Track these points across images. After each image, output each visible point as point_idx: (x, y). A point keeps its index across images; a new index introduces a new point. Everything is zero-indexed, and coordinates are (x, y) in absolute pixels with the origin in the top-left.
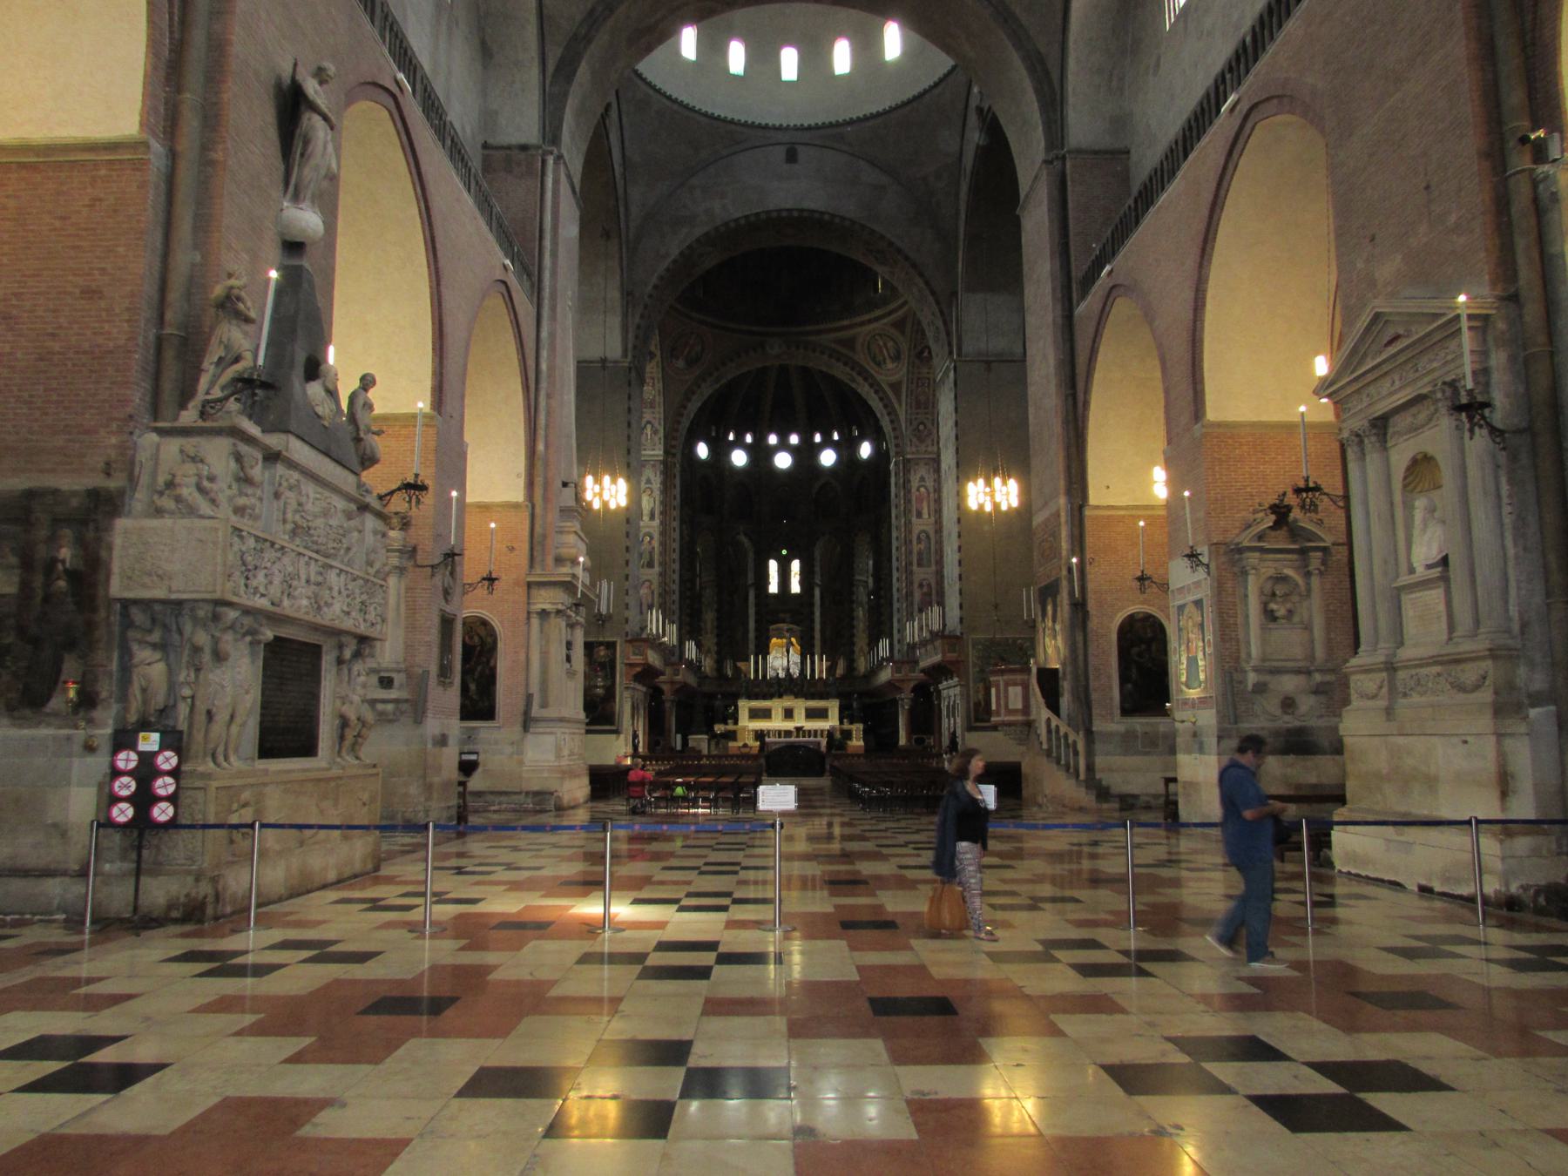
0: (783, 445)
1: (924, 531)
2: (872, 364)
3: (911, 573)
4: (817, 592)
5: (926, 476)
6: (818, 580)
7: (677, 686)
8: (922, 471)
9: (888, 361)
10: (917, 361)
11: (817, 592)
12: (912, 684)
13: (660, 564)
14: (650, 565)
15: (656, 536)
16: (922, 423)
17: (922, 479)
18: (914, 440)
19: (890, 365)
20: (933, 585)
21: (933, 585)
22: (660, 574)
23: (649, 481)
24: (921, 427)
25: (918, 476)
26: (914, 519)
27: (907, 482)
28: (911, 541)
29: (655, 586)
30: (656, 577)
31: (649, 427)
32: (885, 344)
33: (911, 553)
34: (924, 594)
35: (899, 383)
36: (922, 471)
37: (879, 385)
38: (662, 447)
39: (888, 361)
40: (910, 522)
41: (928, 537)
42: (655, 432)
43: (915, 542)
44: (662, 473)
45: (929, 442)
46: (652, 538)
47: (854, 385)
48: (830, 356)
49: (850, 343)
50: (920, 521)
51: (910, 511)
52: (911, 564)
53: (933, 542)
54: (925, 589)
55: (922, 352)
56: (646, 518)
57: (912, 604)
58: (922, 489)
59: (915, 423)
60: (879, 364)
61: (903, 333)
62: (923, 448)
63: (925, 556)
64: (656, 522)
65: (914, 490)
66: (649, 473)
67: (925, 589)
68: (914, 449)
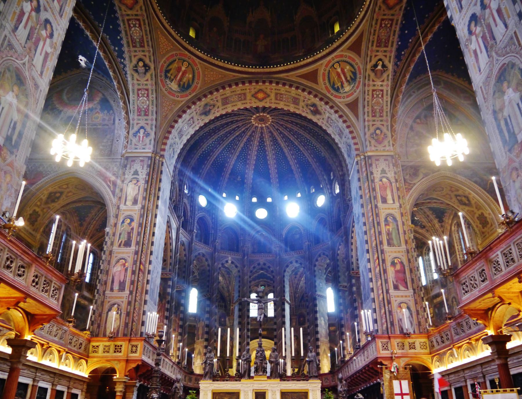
0: (262, 203)
1: (388, 215)
2: (332, 91)
3: (382, 252)
4: (287, 307)
5: (387, 169)
6: (287, 298)
7: (134, 365)
8: (382, 165)
9: (346, 84)
10: (372, 75)
11: (287, 307)
13: (138, 243)
14: (127, 244)
15: (136, 218)
16: (378, 128)
17: (383, 171)
18: (373, 142)
19: (347, 88)
20: (406, 263)
21: (406, 263)
22: (136, 253)
23: (136, 173)
24: (378, 132)
25: (380, 169)
26: (380, 204)
27: (369, 177)
28: (379, 224)
29: (129, 264)
30: (131, 255)
31: (142, 131)
32: (343, 70)
33: (380, 233)
34: (397, 272)
35: (356, 101)
36: (382, 165)
37: (338, 106)
38: (152, 146)
39: (346, 84)
40: (376, 206)
41: (395, 219)
42: (147, 135)
43: (383, 224)
44: (150, 166)
45: (386, 143)
46: (132, 220)
47: (315, 119)
48: (297, 88)
49: (313, 76)
50: (385, 206)
51: (375, 198)
52: (381, 243)
53: (400, 224)
55: (376, 66)
56: (129, 203)
57: (386, 281)
58: (384, 180)
59: (372, 129)
60: (337, 90)
61: (359, 53)
62: (380, 147)
63: (394, 236)
64: (139, 206)
65: (377, 180)
66: (137, 166)
67: (398, 267)
68: (373, 148)
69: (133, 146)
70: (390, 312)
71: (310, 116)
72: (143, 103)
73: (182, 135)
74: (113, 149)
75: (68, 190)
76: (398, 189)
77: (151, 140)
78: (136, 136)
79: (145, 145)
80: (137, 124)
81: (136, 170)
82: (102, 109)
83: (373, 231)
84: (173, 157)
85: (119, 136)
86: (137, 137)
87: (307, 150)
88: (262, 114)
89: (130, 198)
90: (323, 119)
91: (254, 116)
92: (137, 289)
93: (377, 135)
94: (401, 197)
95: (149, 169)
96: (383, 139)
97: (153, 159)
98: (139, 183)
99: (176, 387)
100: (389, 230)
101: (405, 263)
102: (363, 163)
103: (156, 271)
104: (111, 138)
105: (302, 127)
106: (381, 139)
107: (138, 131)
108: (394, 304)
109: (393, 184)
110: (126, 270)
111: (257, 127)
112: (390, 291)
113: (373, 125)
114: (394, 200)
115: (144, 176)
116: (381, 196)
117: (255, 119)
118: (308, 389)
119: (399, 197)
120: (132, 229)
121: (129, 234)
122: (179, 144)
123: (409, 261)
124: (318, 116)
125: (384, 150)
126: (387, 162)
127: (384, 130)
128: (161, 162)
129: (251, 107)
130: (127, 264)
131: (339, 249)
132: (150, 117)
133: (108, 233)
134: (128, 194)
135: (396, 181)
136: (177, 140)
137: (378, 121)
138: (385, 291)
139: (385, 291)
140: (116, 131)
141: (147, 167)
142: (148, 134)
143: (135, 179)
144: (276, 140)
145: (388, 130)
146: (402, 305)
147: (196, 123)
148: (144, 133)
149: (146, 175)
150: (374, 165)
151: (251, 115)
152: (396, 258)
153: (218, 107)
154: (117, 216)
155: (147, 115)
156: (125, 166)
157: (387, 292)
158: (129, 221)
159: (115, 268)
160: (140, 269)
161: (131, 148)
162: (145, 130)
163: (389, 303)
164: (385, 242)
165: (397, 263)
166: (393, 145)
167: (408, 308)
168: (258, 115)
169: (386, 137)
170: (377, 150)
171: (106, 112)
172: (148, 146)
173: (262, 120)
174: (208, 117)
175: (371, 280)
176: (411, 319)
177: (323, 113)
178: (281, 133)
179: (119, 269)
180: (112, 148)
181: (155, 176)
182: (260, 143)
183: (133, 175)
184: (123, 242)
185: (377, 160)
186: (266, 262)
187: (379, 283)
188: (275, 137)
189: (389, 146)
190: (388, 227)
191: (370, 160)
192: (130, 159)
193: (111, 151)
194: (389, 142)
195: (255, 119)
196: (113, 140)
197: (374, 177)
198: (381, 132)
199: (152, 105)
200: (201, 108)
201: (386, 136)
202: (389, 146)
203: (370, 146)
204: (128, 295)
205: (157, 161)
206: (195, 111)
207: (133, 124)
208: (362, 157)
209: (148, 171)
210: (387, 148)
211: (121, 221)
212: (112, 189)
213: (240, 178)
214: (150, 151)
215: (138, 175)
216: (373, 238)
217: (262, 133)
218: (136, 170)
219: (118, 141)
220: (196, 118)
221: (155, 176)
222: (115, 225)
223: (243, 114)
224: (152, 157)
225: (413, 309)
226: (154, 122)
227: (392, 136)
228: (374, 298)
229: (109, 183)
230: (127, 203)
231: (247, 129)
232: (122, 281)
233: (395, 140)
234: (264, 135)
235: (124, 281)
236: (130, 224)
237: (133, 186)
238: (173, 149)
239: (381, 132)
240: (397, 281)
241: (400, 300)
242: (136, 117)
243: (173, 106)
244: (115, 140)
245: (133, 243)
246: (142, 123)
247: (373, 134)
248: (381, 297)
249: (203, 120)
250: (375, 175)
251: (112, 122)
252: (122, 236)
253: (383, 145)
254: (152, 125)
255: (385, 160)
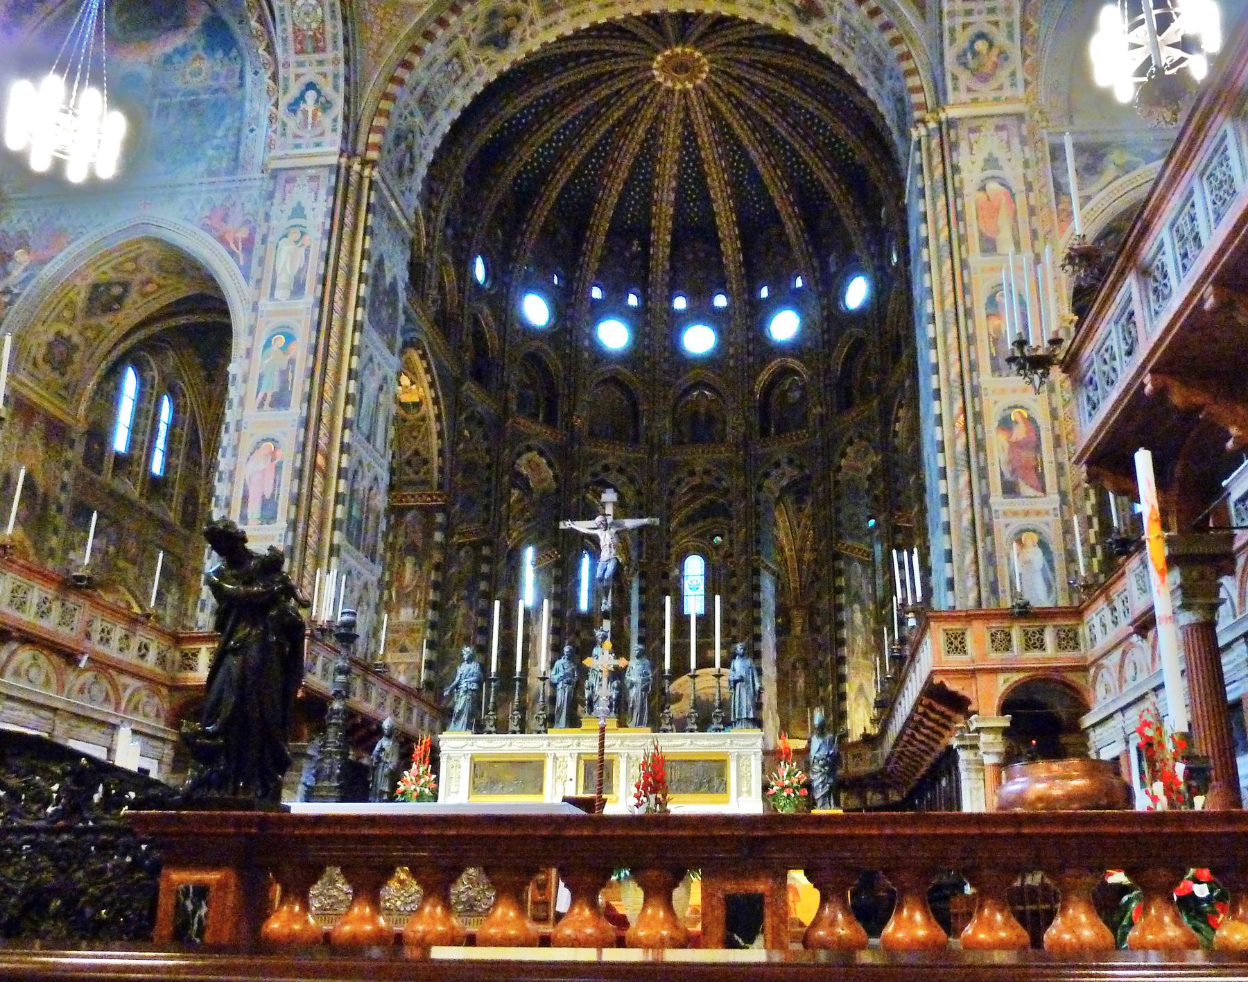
3: (976, 391)
5: (1001, 155)
8: (989, 143)
12: (1001, 685)
14: (280, 401)
16: (981, 36)
17: (991, 162)
20: (1043, 420)
21: (1043, 420)
23: (299, 211)
24: (981, 46)
25: (980, 157)
26: (975, 257)
28: (968, 313)
31: (311, 96)
33: (971, 339)
34: (1016, 446)
36: (989, 143)
40: (964, 264)
42: (326, 106)
45: (1003, 76)
46: (290, 338)
50: (990, 260)
51: (962, 239)
52: (973, 367)
54: (1020, 432)
57: (983, 473)
58: (993, 186)
59: (963, 39)
62: (986, 91)
65: (970, 189)
67: (1020, 432)
68: (964, 96)
69: (290, 140)
70: (991, 557)
71: (796, 29)
72: (307, 14)
73: (434, 108)
74: (241, 154)
75: (139, 277)
76: (1032, 211)
77: (335, 120)
78: (294, 112)
79: (322, 134)
80: (298, 76)
81: (299, 204)
82: (210, 48)
83: (952, 335)
84: (412, 171)
85: (257, 118)
86: (300, 114)
87: (814, 148)
88: (679, 50)
89: (285, 279)
90: (830, 31)
91: (659, 58)
92: (309, 515)
93: (975, 54)
94: (1041, 233)
95: (331, 198)
96: (996, 66)
97: (343, 171)
98: (307, 240)
99: (382, 749)
100: (998, 330)
101: (1039, 421)
102: (935, 142)
103: (369, 476)
104: (237, 124)
105: (792, 77)
106: (987, 69)
107: (302, 98)
108: (1003, 534)
109: (1020, 198)
110: (278, 468)
111: (670, 92)
112: (991, 500)
113: (965, 26)
114: (1017, 244)
115: (320, 219)
116: (981, 235)
117: (662, 68)
118: (726, 754)
119: (1034, 234)
120: (292, 362)
121: (284, 374)
122: (427, 135)
123: (1054, 414)
124: (816, 24)
125: (997, 100)
126: (1004, 134)
127: (1000, 38)
128: (366, 183)
129: (629, 17)
130: (279, 453)
131: (897, 420)
132: (329, 55)
133: (234, 377)
134: (279, 268)
135: (1029, 187)
136: (418, 119)
137: (980, 13)
138: (977, 501)
139: (977, 501)
140: (247, 104)
141: (328, 194)
142: (328, 102)
143: (297, 230)
144: (729, 126)
145: (1011, 36)
146: (1024, 536)
147: (473, 71)
148: (317, 101)
149: (325, 215)
150: (963, 146)
151: (649, 54)
152: (1016, 407)
153: (531, 22)
154: (252, 331)
155: (323, 50)
156: (271, 196)
157: (985, 501)
158: (282, 340)
159: (251, 464)
160: (314, 465)
161: (283, 147)
162: (319, 92)
163: (989, 531)
164: (985, 364)
165: (1016, 422)
166: (1027, 83)
167: (1043, 545)
168: (668, 53)
169: (1006, 59)
170: (975, 100)
171: (219, 54)
172: (329, 136)
173: (682, 67)
174: (507, 52)
175: (943, 474)
176: (1050, 576)
177: (827, 11)
178: (739, 104)
179: (261, 466)
180: (237, 152)
181: (348, 220)
182: (684, 139)
183: (290, 218)
184: (269, 398)
185: (973, 130)
186: (708, 466)
187: (964, 479)
188: (723, 119)
189: (1013, 85)
190: (995, 322)
191: (952, 132)
192: (283, 176)
193: (236, 159)
194: (1013, 74)
195: (662, 68)
196: (240, 130)
197: (961, 182)
198: (991, 45)
199: (333, 17)
200: (480, 25)
201: (1004, 56)
202: (1013, 85)
203: (955, 89)
204: (283, 533)
205: (354, 179)
206: (463, 31)
207: (286, 79)
208: (932, 125)
209: (330, 204)
210: (1007, 92)
211: (263, 342)
212: (242, 263)
213: (639, 245)
214: (336, 149)
215: (305, 217)
216: (954, 356)
217: (687, 109)
218: (299, 204)
219: (252, 130)
220: (468, 54)
221: (348, 220)
222: (249, 353)
223: (625, 54)
224: (339, 167)
225: (1057, 548)
226: (341, 68)
227: (1025, 57)
228: (948, 523)
229: (233, 246)
230: (278, 294)
231: (644, 99)
232: (268, 496)
233: (1034, 69)
234: (693, 116)
235: (273, 495)
236: (284, 349)
237: (292, 247)
238: (410, 148)
239: (991, 45)
240: (1013, 472)
241: (1018, 522)
242: (293, 58)
243: (395, 21)
244: (246, 130)
245: (296, 397)
246: (310, 74)
247: (965, 54)
248: (967, 517)
249: (491, 63)
250: (965, 174)
251: (236, 81)
252: (265, 381)
253: (994, 84)
254: (336, 76)
255: (999, 128)
